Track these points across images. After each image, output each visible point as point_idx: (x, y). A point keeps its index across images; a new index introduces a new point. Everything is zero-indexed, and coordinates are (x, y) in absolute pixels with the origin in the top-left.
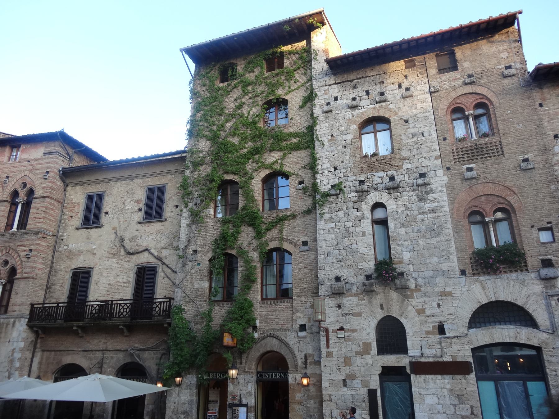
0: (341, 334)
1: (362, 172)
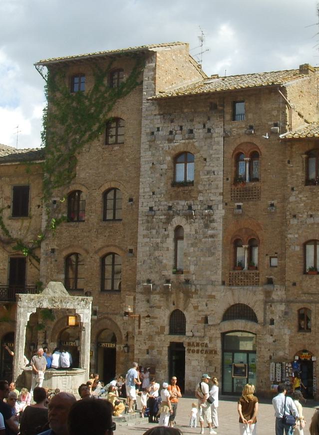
0: (148, 320)
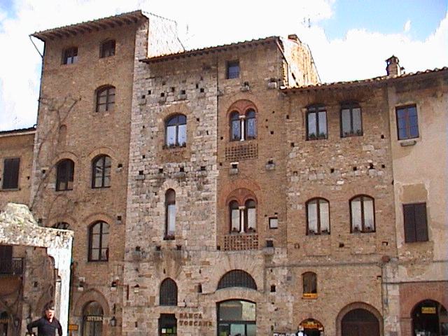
0: (136, 290)
1: (162, 161)
